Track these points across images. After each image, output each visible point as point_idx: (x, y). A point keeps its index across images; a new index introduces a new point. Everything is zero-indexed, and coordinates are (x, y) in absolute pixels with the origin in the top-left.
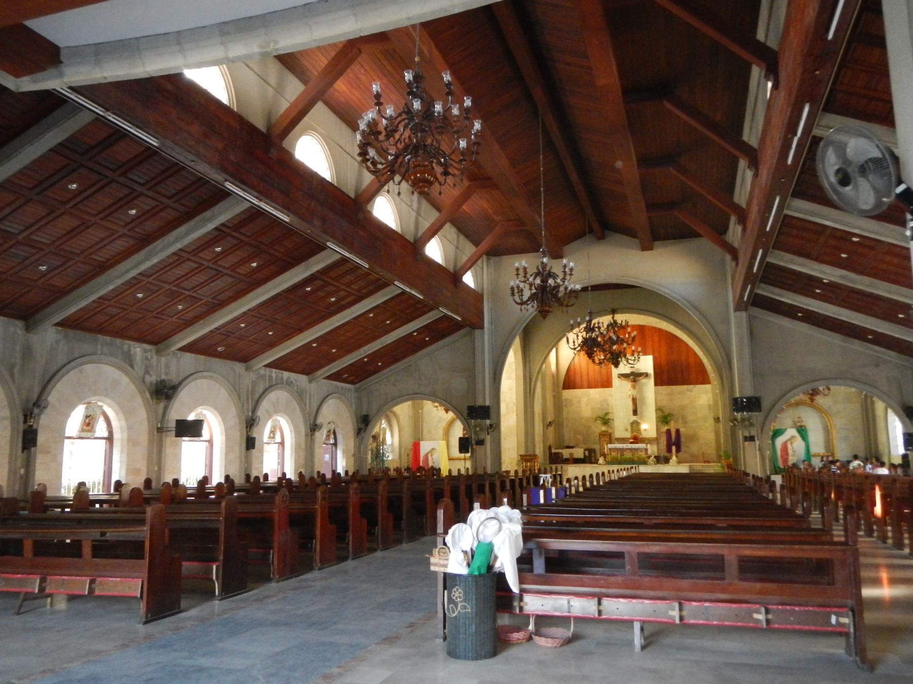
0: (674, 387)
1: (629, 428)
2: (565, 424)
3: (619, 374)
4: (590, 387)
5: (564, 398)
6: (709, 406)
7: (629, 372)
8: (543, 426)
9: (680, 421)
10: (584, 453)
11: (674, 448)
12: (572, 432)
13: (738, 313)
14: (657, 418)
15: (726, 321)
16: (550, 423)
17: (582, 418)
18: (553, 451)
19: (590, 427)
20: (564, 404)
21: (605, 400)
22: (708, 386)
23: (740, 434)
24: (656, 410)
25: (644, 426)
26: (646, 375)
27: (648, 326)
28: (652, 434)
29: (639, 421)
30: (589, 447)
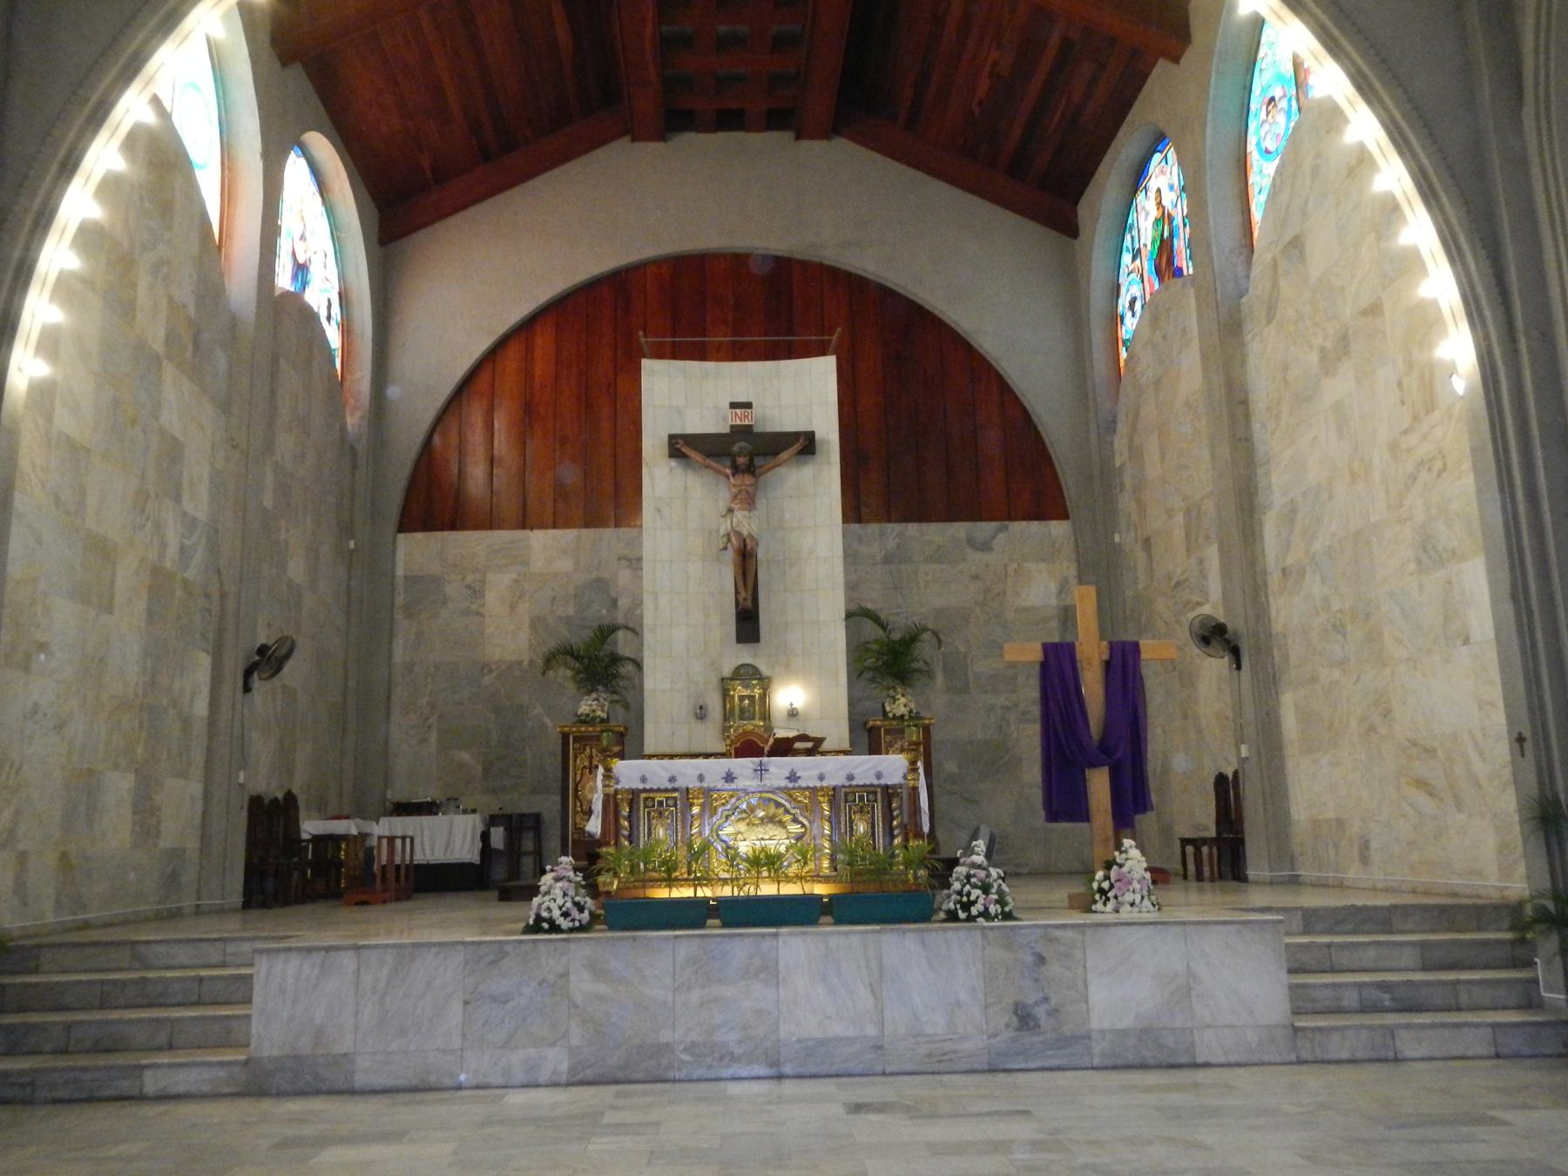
0: (913, 528)
1: (714, 702)
2: (399, 693)
3: (671, 437)
4: (524, 523)
5: (400, 572)
7: (727, 430)
8: (217, 668)
9: (940, 679)
10: (485, 837)
11: (1099, 784)
12: (433, 737)
14: (858, 653)
16: (262, 650)
17: (486, 668)
18: (310, 827)
20: (400, 600)
21: (600, 585)
22: (1058, 528)
24: (849, 615)
26: (806, 445)
27: (804, 264)
28: (837, 732)
29: (765, 670)
30: (509, 810)
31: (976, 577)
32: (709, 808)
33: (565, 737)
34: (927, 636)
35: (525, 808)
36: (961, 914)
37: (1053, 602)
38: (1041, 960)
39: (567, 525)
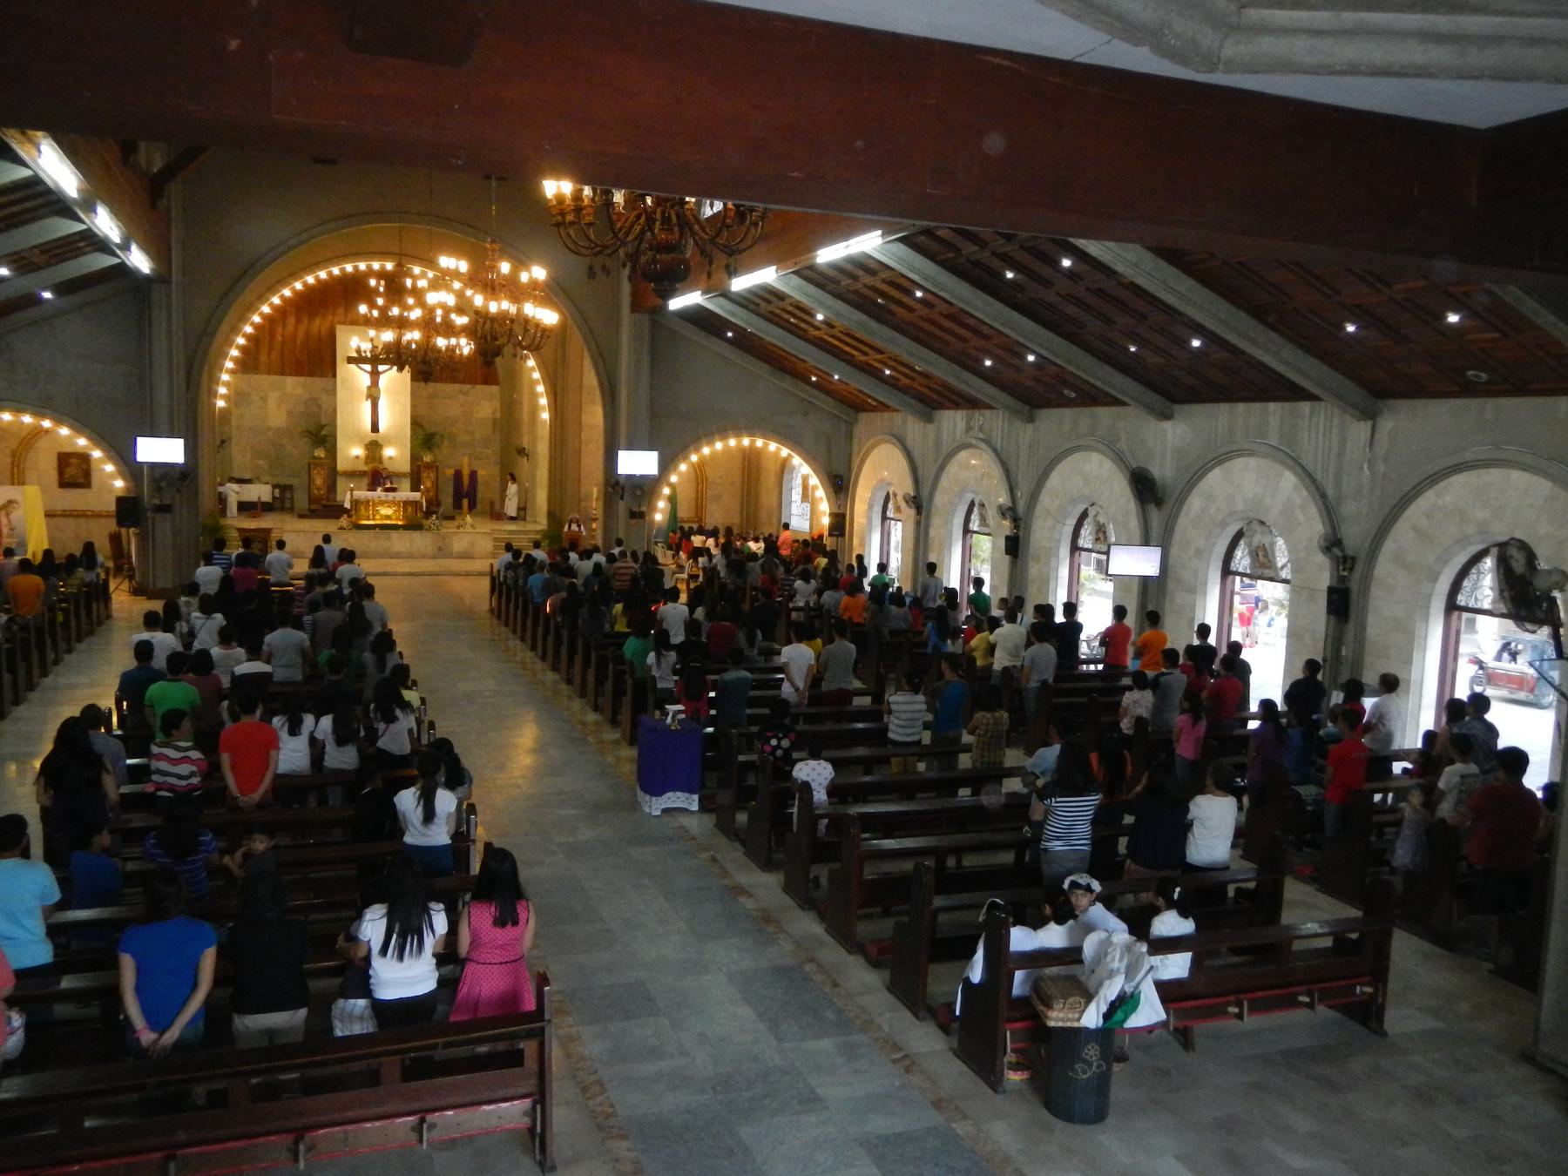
4: (283, 373)
6: (495, 422)
10: (273, 493)
11: (465, 502)
12: (249, 455)
13: (637, 315)
15: (613, 321)
17: (269, 429)
19: (282, 446)
21: (315, 400)
22: (495, 389)
23: (622, 507)
25: (389, 452)
28: (405, 466)
31: (462, 406)
32: (375, 504)
33: (309, 464)
34: (437, 437)
35: (288, 483)
36: (429, 529)
37: (490, 416)
38: (444, 539)
39: (302, 375)
